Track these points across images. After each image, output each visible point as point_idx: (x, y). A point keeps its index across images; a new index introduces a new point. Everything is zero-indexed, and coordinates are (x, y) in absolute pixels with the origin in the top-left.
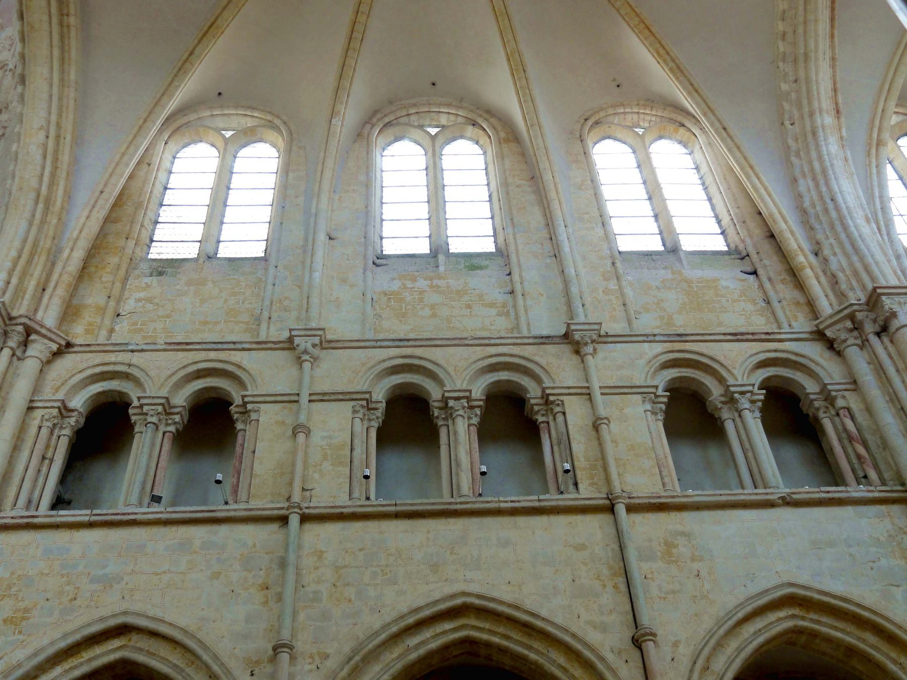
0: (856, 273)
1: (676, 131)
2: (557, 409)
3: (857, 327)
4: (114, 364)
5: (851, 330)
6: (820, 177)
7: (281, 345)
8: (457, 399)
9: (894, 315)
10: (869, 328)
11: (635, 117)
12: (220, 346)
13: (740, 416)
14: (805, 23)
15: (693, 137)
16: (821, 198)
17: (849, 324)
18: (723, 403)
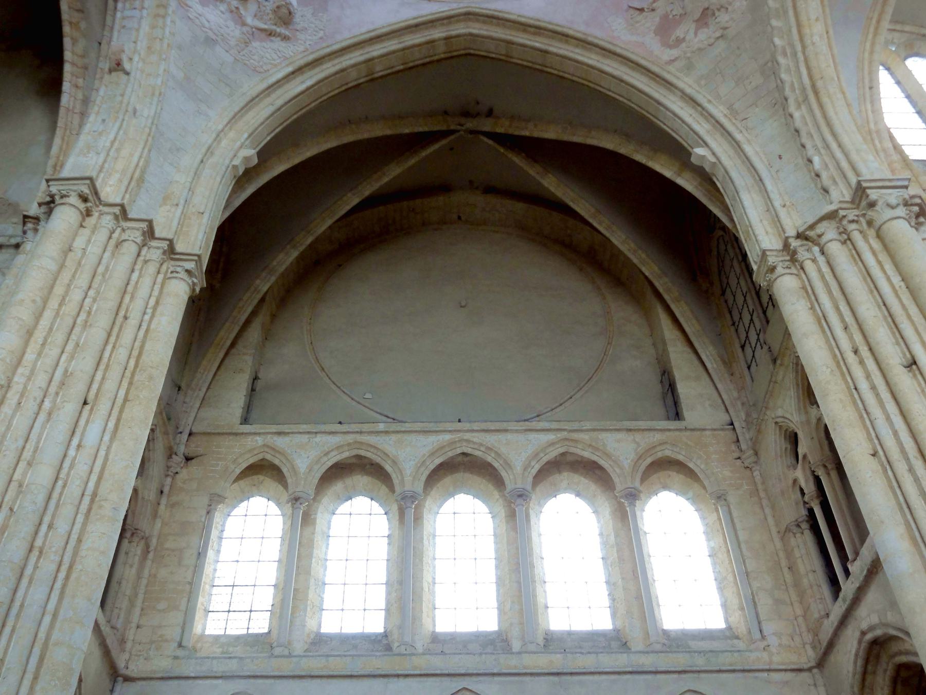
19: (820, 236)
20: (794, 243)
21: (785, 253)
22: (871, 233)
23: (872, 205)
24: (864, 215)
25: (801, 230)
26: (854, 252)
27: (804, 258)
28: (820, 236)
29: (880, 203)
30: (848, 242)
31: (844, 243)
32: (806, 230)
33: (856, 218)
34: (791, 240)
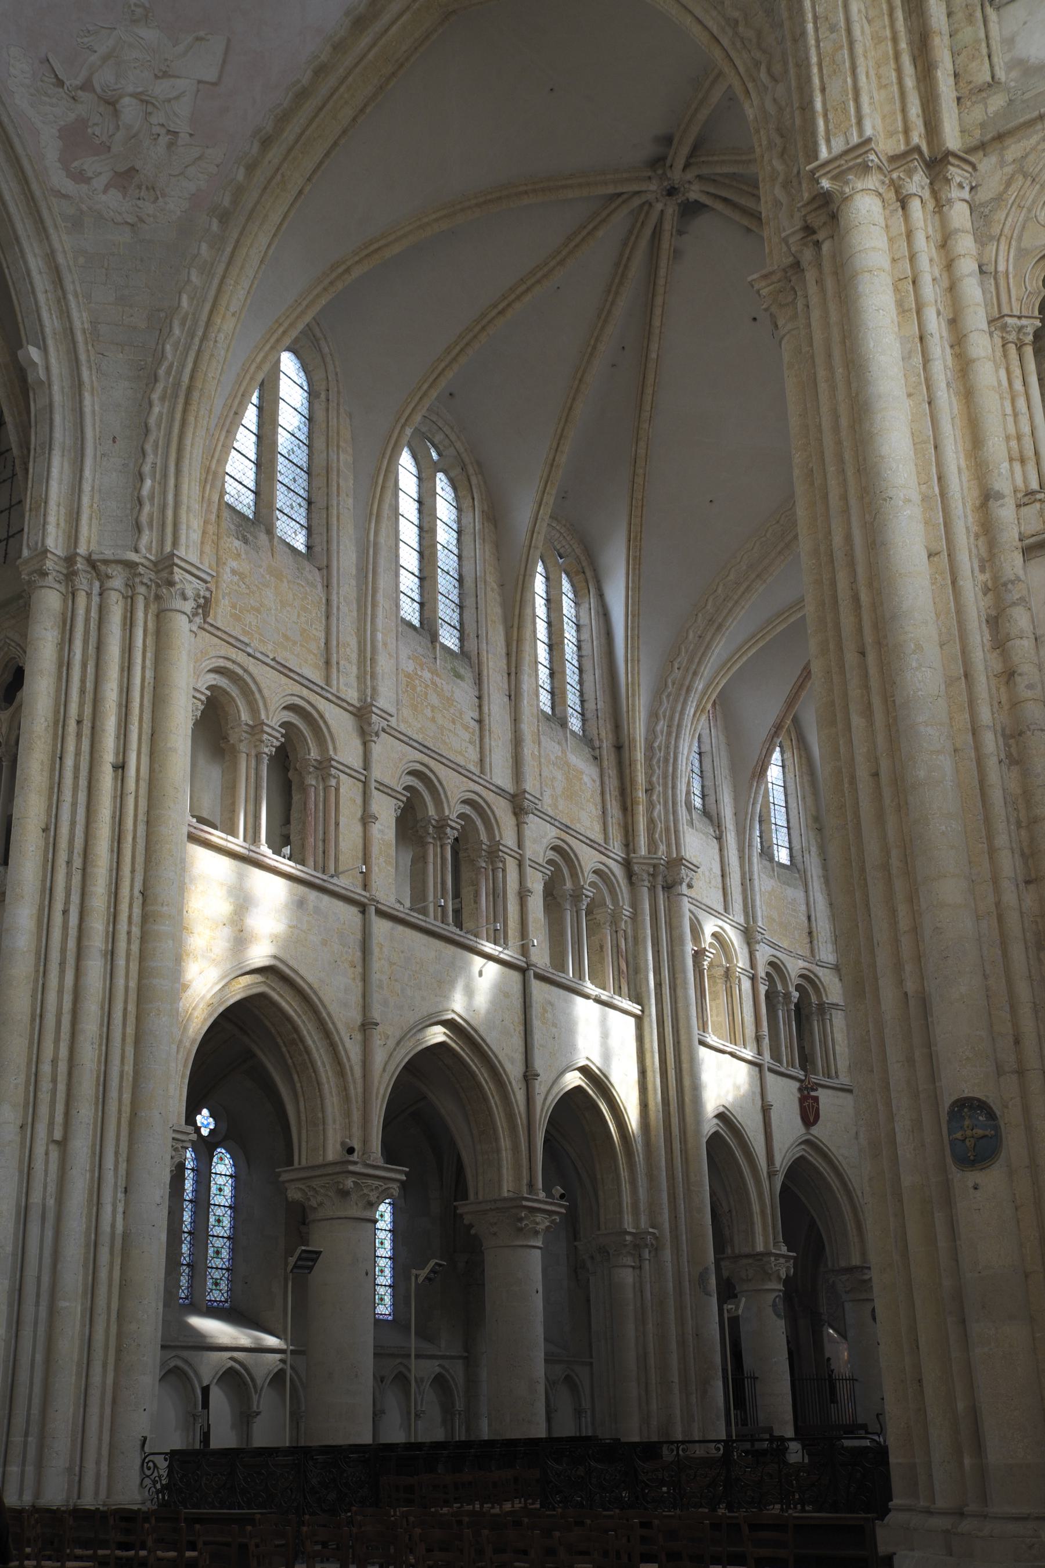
0: (667, 829)
1: (577, 573)
2: (501, 865)
3: (654, 875)
4: (234, 662)
5: (649, 874)
6: (674, 729)
7: (350, 708)
8: (452, 828)
9: (681, 884)
10: (660, 879)
11: (558, 535)
12: (311, 686)
13: (577, 912)
14: (736, 602)
15: (587, 591)
16: (667, 747)
17: (652, 870)
18: (571, 896)
19: (108, 577)
20: (80, 565)
21: (62, 563)
22: (153, 608)
23: (171, 583)
24: (158, 586)
25: (94, 557)
26: (129, 615)
27: (82, 587)
28: (108, 577)
29: (178, 587)
30: (129, 600)
31: (125, 598)
32: (99, 561)
33: (149, 583)
34: (79, 559)
